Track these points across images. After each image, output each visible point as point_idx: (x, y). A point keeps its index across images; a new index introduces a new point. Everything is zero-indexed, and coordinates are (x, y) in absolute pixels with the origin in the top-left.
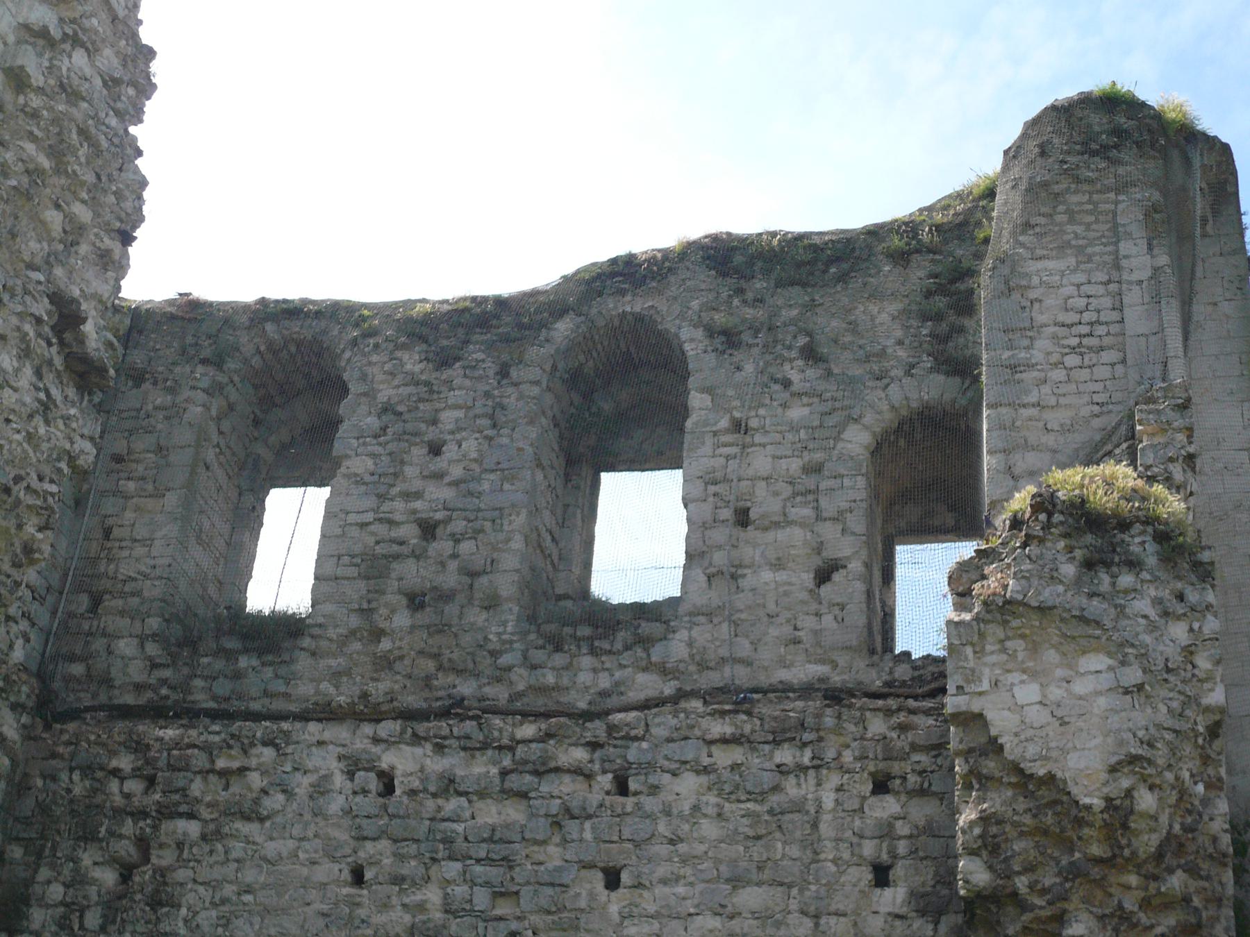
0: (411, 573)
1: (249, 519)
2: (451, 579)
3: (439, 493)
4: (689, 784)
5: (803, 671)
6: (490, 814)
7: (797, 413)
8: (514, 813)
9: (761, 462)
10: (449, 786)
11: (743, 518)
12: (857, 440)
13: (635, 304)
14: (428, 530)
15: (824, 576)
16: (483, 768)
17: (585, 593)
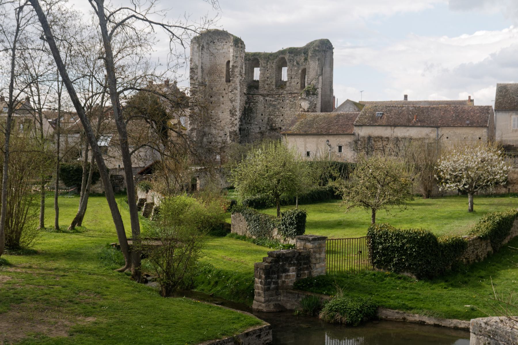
0: (266, 82)
1: (253, 72)
2: (269, 83)
3: (268, 75)
4: (287, 101)
5: (296, 91)
6: (274, 103)
7: (296, 68)
8: (276, 103)
9: (293, 73)
10: (271, 101)
11: (291, 78)
12: (300, 71)
13: (283, 56)
14: (268, 78)
15: (297, 83)
16: (273, 99)
17: (281, 80)
